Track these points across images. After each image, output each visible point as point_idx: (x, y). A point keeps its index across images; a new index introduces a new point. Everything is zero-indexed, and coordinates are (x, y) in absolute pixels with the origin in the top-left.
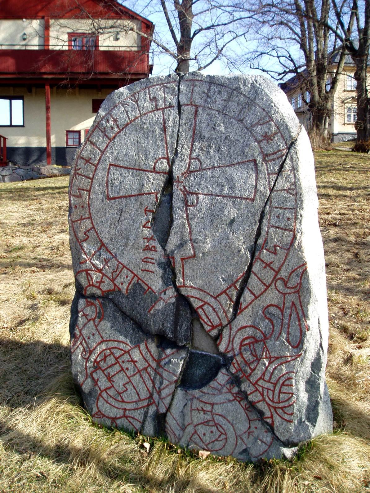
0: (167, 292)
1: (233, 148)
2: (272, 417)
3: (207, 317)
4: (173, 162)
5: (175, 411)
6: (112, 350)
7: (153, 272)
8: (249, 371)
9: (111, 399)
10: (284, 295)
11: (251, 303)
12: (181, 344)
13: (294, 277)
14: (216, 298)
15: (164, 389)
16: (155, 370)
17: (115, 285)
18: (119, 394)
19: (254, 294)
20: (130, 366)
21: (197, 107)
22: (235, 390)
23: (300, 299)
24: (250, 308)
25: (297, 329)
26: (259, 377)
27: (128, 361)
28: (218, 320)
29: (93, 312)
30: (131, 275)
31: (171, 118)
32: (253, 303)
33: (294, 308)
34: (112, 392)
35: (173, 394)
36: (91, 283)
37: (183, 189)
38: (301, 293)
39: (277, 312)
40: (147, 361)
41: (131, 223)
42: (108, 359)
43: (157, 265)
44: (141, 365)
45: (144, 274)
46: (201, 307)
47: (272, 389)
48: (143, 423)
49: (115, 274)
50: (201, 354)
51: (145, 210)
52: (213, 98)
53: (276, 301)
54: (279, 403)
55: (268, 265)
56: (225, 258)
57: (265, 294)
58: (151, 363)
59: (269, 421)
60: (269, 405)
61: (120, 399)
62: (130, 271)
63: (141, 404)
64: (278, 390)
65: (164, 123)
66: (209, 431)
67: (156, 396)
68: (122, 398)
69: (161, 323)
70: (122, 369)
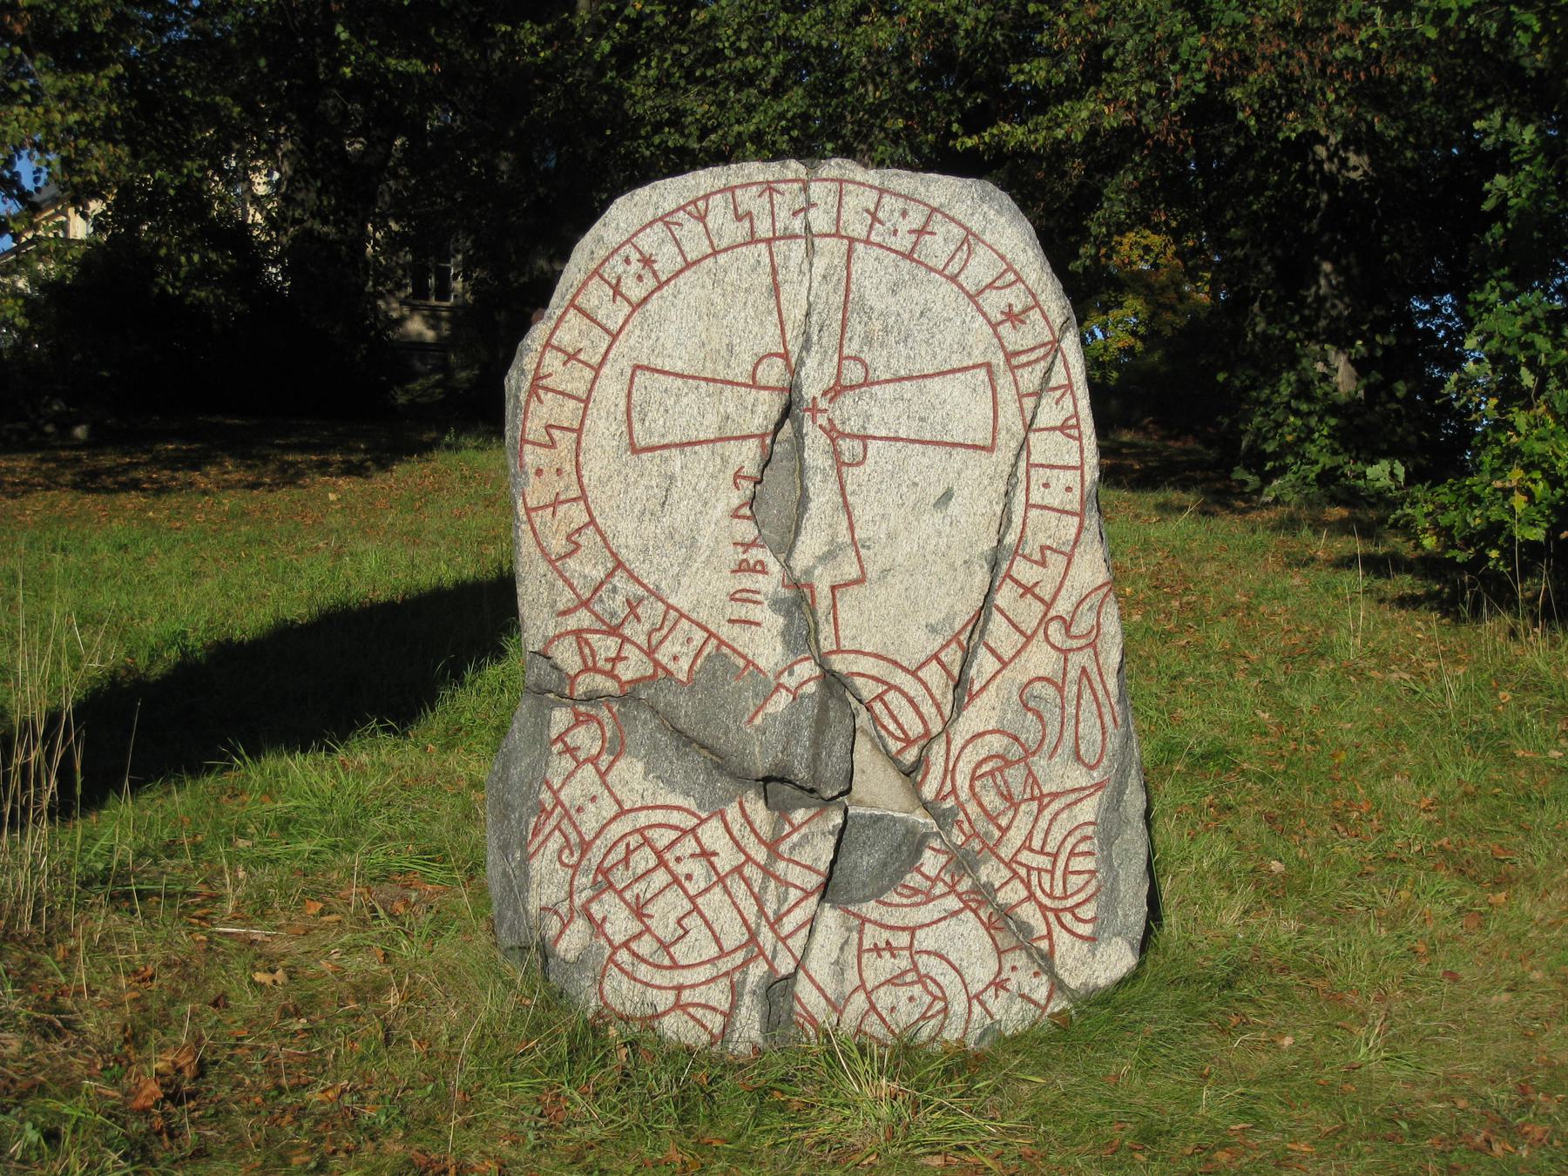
0: (796, 668)
1: (939, 336)
2: (1049, 935)
4: (801, 362)
5: (819, 965)
6: (649, 833)
7: (758, 624)
8: (997, 834)
9: (643, 967)
10: (1065, 652)
11: (994, 677)
12: (829, 794)
14: (914, 674)
15: (789, 911)
17: (657, 664)
18: (665, 946)
19: (999, 658)
20: (698, 868)
21: (852, 240)
22: (965, 885)
24: (992, 688)
26: (1019, 843)
27: (692, 856)
29: (593, 739)
30: (699, 636)
31: (792, 264)
33: (1085, 681)
34: (645, 946)
36: (590, 664)
37: (828, 427)
39: (1050, 691)
40: (741, 849)
41: (699, 507)
42: (635, 857)
44: (724, 863)
45: (737, 628)
46: (880, 697)
48: (729, 1016)
51: (737, 476)
52: (888, 224)
54: (1066, 897)
55: (1028, 590)
56: (935, 580)
57: (1024, 655)
58: (752, 853)
59: (1044, 945)
61: (667, 962)
62: (698, 625)
66: (904, 999)
67: (766, 937)
68: (672, 958)
69: (780, 747)
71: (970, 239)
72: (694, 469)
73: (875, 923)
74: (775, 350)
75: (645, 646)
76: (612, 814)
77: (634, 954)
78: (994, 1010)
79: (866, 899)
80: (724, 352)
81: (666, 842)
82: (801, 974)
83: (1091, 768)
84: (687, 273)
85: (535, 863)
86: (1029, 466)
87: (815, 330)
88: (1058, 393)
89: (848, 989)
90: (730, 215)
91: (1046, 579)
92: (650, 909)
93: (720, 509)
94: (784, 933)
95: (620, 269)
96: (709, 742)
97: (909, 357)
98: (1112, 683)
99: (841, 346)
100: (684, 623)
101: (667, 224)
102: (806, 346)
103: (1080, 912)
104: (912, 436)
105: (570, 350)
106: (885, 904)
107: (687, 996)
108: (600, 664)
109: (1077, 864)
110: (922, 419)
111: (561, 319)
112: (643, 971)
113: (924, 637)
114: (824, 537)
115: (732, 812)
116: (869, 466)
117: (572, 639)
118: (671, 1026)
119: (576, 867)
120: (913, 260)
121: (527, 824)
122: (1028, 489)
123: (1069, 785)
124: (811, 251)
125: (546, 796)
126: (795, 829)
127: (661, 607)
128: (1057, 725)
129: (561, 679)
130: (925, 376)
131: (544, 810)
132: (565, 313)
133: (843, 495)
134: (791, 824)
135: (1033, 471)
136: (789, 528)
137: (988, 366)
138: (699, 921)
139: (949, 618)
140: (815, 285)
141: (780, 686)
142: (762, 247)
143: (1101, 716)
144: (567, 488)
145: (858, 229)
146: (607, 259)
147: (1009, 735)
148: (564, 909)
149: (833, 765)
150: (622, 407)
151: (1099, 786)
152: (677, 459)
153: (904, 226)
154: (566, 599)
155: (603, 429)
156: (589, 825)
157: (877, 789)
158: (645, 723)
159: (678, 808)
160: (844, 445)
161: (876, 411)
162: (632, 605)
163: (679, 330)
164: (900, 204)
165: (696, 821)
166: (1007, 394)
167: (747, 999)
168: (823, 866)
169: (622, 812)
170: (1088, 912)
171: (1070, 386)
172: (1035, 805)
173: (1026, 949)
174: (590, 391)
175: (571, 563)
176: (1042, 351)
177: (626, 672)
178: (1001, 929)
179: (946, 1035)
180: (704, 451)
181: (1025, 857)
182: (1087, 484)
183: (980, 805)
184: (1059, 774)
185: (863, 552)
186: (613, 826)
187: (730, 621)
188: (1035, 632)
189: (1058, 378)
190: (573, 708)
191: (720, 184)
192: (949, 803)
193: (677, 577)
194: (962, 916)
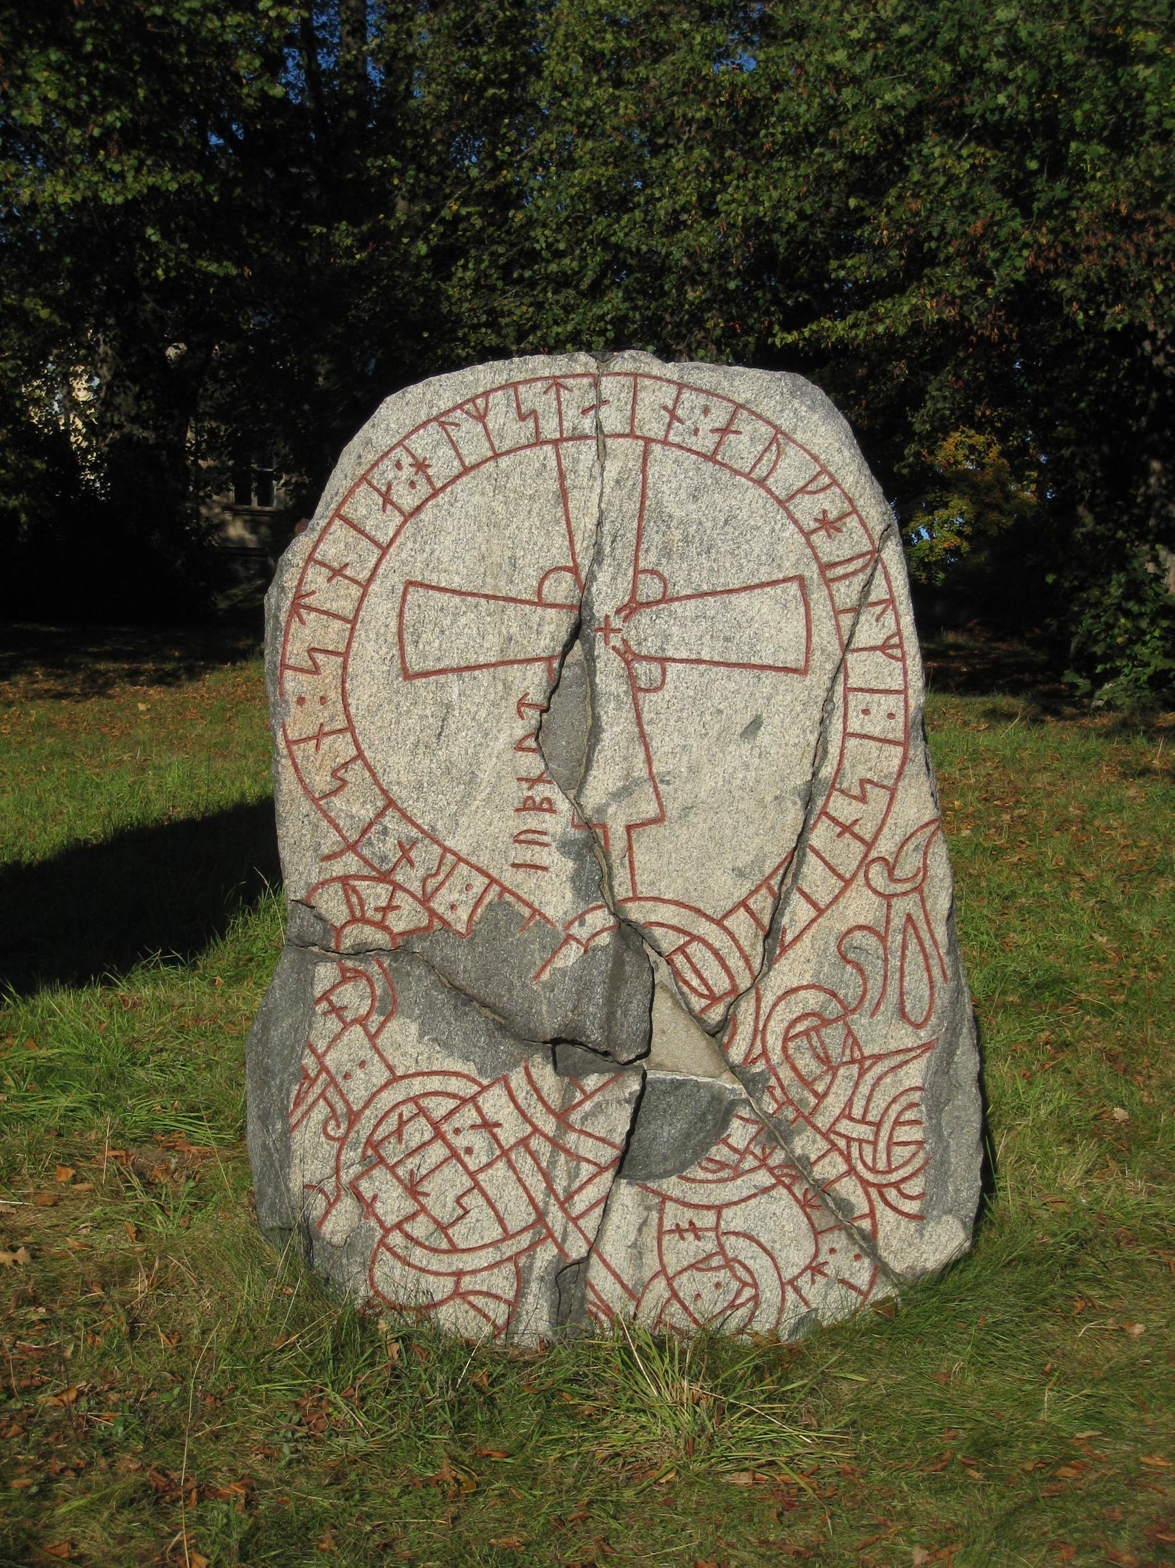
2: (872, 1214)
4: (592, 577)
5: (615, 1249)
6: (424, 1103)
7: (545, 869)
8: (813, 1101)
9: (418, 1251)
10: (888, 897)
11: (808, 926)
12: (625, 1057)
14: (719, 923)
15: (581, 1188)
16: (552, 1141)
17: (432, 913)
18: (442, 1228)
19: (814, 905)
20: (479, 1141)
21: (648, 441)
22: (778, 1157)
24: (807, 939)
26: (837, 1111)
27: (473, 1127)
29: (362, 998)
30: (479, 882)
33: (911, 930)
34: (420, 1228)
35: (606, 1201)
36: (358, 914)
37: (622, 648)
39: (871, 942)
40: (526, 1119)
42: (409, 1129)
44: (509, 1134)
45: (521, 874)
46: (681, 949)
48: (514, 1305)
49: (431, 884)
51: (521, 703)
53: (870, 917)
54: (890, 1171)
55: (846, 829)
57: (843, 901)
59: (866, 1224)
60: (865, 1183)
61: (445, 1245)
62: (478, 869)
63: (509, 1248)
65: (562, 477)
67: (555, 1217)
68: (450, 1241)
69: (570, 1006)
70: (454, 1154)
71: (779, 438)
72: (472, 698)
74: (562, 563)
75: (419, 894)
77: (408, 1236)
78: (810, 1297)
79: (667, 1174)
80: (506, 567)
81: (443, 1111)
82: (594, 1259)
83: (918, 1026)
84: (465, 479)
85: (297, 1135)
86: (847, 690)
87: (607, 540)
88: (879, 609)
89: (648, 1275)
90: (513, 414)
91: (866, 816)
92: (426, 1187)
93: (502, 742)
94: (575, 1212)
95: (390, 475)
96: (491, 1000)
97: (711, 570)
98: (941, 933)
99: (637, 558)
101: (442, 424)
102: (598, 559)
103: (907, 1188)
104: (717, 658)
105: (335, 565)
106: (688, 1179)
107: (467, 1283)
108: (370, 914)
109: (904, 1134)
110: (727, 639)
111: (325, 530)
112: (418, 1256)
113: (730, 882)
114: (618, 771)
115: (517, 1078)
116: (667, 693)
117: (338, 886)
118: (447, 1316)
119: (342, 1140)
120: (716, 462)
122: (845, 716)
123: (893, 1046)
124: (602, 453)
125: (309, 1061)
126: (587, 1097)
127: (436, 850)
128: (880, 979)
130: (730, 591)
131: (307, 1077)
132: (329, 524)
133: (640, 724)
134: (583, 1091)
135: (851, 696)
136: (579, 761)
137: (800, 579)
138: (481, 1201)
139: (759, 860)
140: (607, 490)
141: (570, 937)
142: (548, 449)
143: (928, 969)
144: (332, 718)
145: (655, 429)
146: (376, 464)
147: (826, 991)
148: (329, 1186)
149: (629, 1025)
150: (393, 628)
151: (927, 1047)
152: (454, 686)
153: (706, 425)
155: (372, 651)
156: (357, 1092)
157: (679, 1051)
158: (419, 979)
159: (457, 1074)
160: (641, 668)
161: (677, 631)
163: (456, 542)
164: (701, 400)
165: (476, 1088)
166: (821, 610)
167: (534, 1286)
168: (619, 1138)
169: (394, 1079)
170: (914, 1187)
171: (892, 601)
172: (855, 1069)
173: (846, 1229)
174: (358, 610)
175: (337, 802)
176: (860, 562)
177: (399, 923)
178: (818, 1207)
179: (756, 1326)
180: (483, 676)
181: (844, 1126)
182: (912, 710)
183: (794, 1068)
184: (882, 1033)
185: (661, 787)
186: (384, 1095)
187: (514, 865)
188: (854, 876)
189: (879, 592)
190: (339, 963)
191: (501, 379)
192: (760, 1067)
194: (774, 1193)
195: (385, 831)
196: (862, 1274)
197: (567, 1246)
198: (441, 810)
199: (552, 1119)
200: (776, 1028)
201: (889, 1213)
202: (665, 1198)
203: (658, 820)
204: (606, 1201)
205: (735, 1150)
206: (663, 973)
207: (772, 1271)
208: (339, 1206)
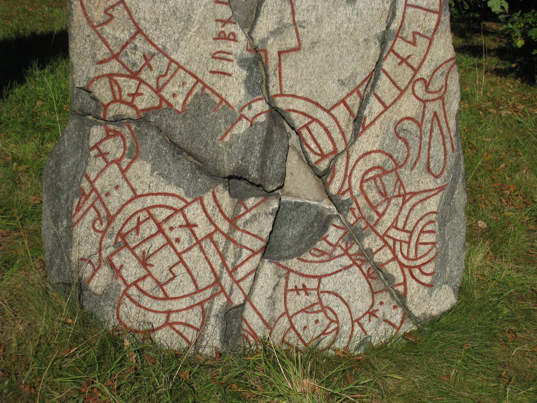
2: (405, 283)
3: (316, 142)
5: (260, 300)
6: (153, 211)
7: (229, 75)
8: (376, 217)
10: (424, 102)
11: (379, 116)
12: (270, 188)
13: (438, 76)
14: (328, 112)
15: (242, 264)
16: (227, 236)
17: (162, 99)
18: (160, 285)
19: (383, 104)
20: (184, 235)
22: (354, 249)
23: (444, 108)
24: (378, 123)
25: (440, 150)
26: (389, 224)
27: (181, 226)
28: (332, 146)
29: (118, 147)
30: (191, 81)
32: (383, 115)
33: (435, 121)
34: (147, 285)
35: (256, 272)
36: (118, 97)
38: (446, 98)
39: (413, 127)
42: (143, 226)
43: (238, 63)
44: (201, 232)
45: (215, 77)
46: (306, 126)
47: (407, 240)
48: (200, 331)
49: (162, 81)
50: (295, 203)
53: (414, 112)
54: (416, 259)
55: (404, 61)
58: (220, 226)
59: (401, 289)
60: (402, 265)
61: (161, 295)
62: (190, 73)
63: (199, 298)
64: (415, 240)
66: (312, 322)
67: (226, 281)
68: (165, 293)
69: (240, 157)
73: (296, 272)
75: (155, 87)
76: (129, 198)
79: (290, 257)
81: (163, 217)
82: (248, 305)
83: (436, 177)
89: (277, 314)
91: (414, 53)
92: (152, 261)
96: (194, 151)
98: (452, 124)
100: (181, 72)
106: (303, 260)
107: (173, 317)
108: (125, 97)
112: (146, 301)
113: (336, 88)
114: (275, 18)
115: (208, 198)
117: (106, 80)
118: (165, 337)
119: (104, 232)
121: (72, 203)
123: (422, 187)
125: (85, 185)
126: (248, 211)
127: (166, 60)
128: (417, 148)
129: (98, 107)
131: (84, 194)
134: (245, 207)
136: (252, 11)
138: (184, 270)
139: (354, 75)
141: (242, 116)
143: (444, 144)
147: (387, 154)
148: (95, 260)
149: (273, 170)
151: (441, 189)
154: (103, 52)
156: (113, 204)
157: (300, 185)
158: (153, 137)
159: (173, 195)
162: (147, 59)
165: (184, 204)
167: (212, 320)
170: (429, 269)
172: (400, 200)
175: (107, 29)
177: (142, 104)
178: (375, 278)
179: (337, 345)
181: (393, 233)
183: (367, 198)
184: (417, 180)
185: (300, 30)
186: (129, 206)
187: (212, 72)
188: (406, 88)
190: (105, 126)
193: (177, 41)
194: (351, 269)
195: (135, 48)
196: (397, 316)
197: (232, 298)
198: (170, 36)
199: (227, 223)
200: (357, 175)
201: (414, 283)
202: (289, 271)
203: (297, 49)
204: (256, 272)
205: (330, 244)
206: (294, 139)
207: (348, 314)
208: (100, 271)
